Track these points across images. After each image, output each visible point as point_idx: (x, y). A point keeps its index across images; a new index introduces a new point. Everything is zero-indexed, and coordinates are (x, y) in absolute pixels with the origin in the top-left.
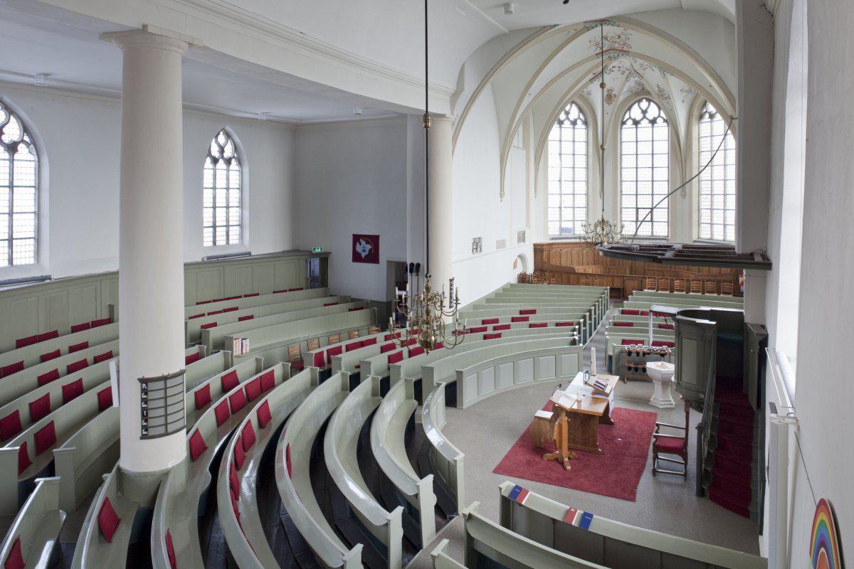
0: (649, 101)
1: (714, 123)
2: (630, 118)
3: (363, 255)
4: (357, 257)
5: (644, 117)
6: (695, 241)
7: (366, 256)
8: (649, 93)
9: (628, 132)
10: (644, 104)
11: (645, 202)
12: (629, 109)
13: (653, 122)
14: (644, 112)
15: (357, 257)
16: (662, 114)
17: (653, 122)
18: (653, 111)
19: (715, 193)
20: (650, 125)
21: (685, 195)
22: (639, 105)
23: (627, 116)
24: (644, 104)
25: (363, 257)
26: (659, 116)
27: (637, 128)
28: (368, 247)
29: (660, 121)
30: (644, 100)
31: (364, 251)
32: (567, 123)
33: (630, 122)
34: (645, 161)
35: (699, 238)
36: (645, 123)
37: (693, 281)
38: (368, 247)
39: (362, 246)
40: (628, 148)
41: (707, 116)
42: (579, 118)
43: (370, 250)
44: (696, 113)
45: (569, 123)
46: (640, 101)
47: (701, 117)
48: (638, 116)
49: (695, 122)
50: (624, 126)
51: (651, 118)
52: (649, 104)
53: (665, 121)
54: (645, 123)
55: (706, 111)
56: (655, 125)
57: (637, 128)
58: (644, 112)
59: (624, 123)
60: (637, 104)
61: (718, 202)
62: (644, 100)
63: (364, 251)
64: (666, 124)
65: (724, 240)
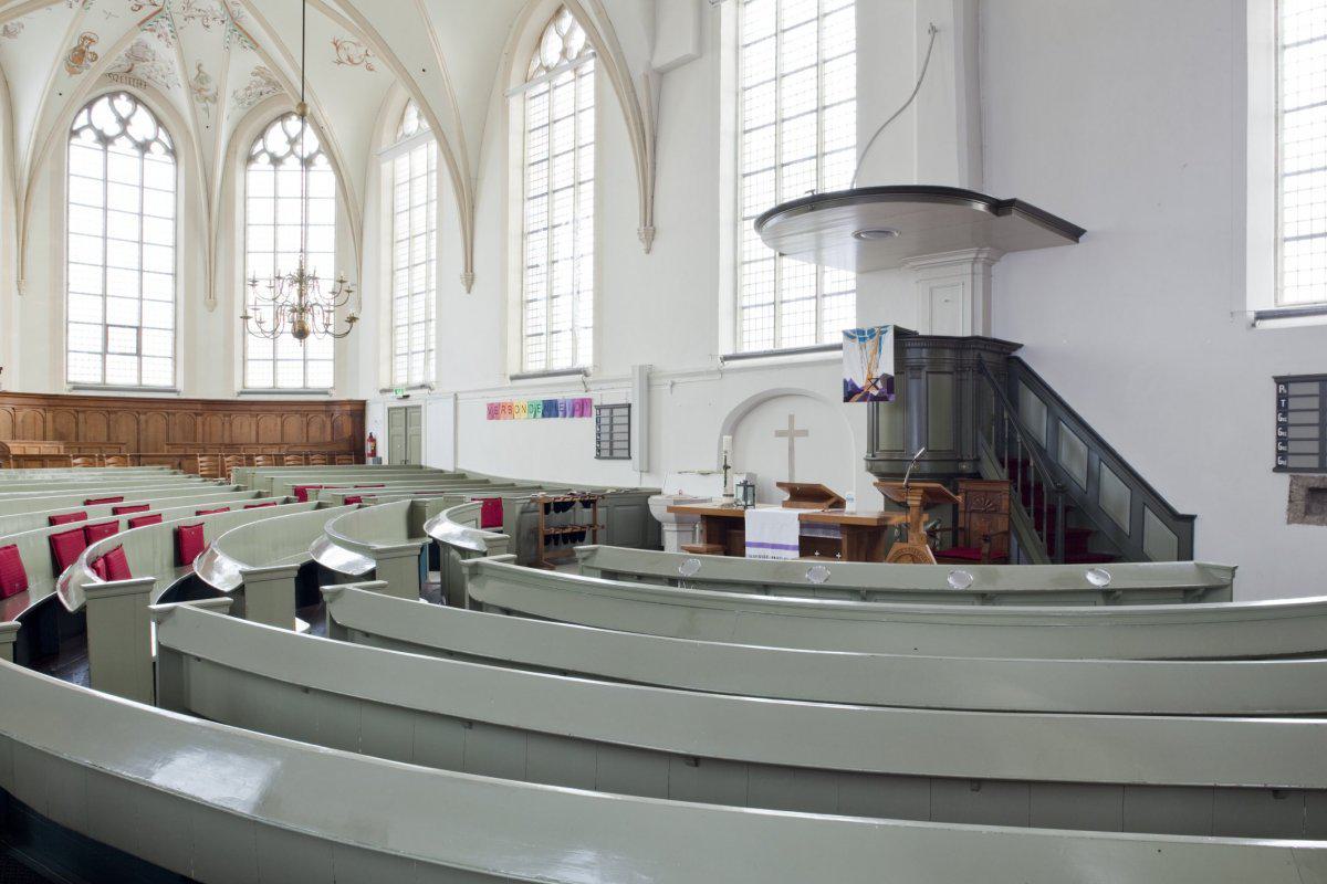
0: (136, 100)
1: (280, 174)
2: (90, 125)
5: (124, 132)
6: (242, 393)
8: (141, 84)
9: (82, 155)
10: (124, 105)
11: (122, 312)
12: (89, 105)
13: (144, 147)
14: (124, 122)
16: (162, 135)
17: (144, 147)
18: (143, 125)
20: (136, 153)
21: (215, 304)
22: (111, 104)
23: (82, 120)
26: (156, 139)
27: (105, 150)
29: (155, 147)
30: (123, 97)
32: (292, 163)
33: (88, 137)
34: (124, 226)
35: (244, 387)
40: (82, 190)
41: (264, 159)
42: (156, 139)
44: (242, 149)
45: (130, 144)
46: (113, 95)
47: (250, 159)
48: (112, 128)
49: (239, 165)
50: (74, 141)
51: (140, 139)
52: (135, 110)
53: (173, 152)
54: (123, 145)
55: (264, 150)
56: (147, 155)
57: (105, 150)
58: (124, 122)
59: (74, 133)
60: (106, 100)
62: (123, 97)
64: (169, 159)
65: (274, 387)
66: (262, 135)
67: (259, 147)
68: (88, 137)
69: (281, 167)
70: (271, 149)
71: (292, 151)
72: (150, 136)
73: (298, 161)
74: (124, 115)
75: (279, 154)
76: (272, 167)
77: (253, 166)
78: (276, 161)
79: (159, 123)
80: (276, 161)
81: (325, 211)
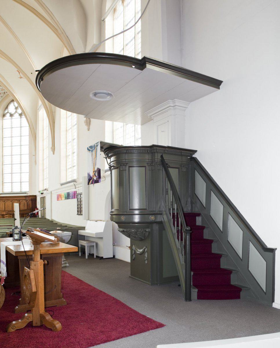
1: (13, 120)
19: (13, 163)
35: (3, 192)
37: (6, 215)
41: (8, 115)
47: (4, 116)
55: (8, 112)
61: (16, 168)
66: (7, 108)
67: (6, 111)
69: (13, 117)
70: (10, 112)
71: (16, 112)
73: (18, 115)
75: (13, 113)
76: (10, 118)
77: (5, 118)
78: (11, 115)
80: (11, 115)
81: (26, 130)
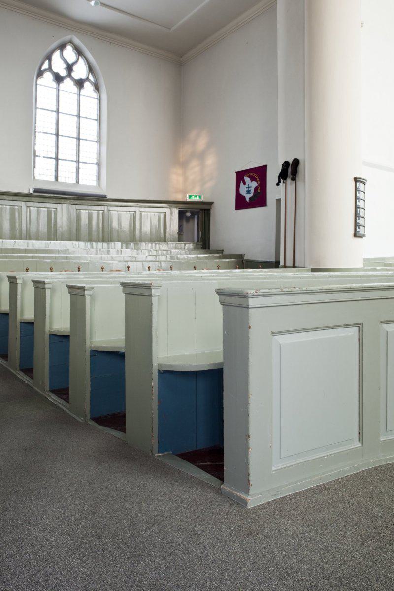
0: (79, 52)
3: (248, 197)
4: (241, 203)
5: (69, 75)
7: (251, 198)
14: (70, 68)
15: (241, 203)
16: (91, 78)
17: (80, 83)
18: (80, 70)
23: (45, 66)
24: (69, 53)
25: (247, 200)
28: (254, 184)
29: (87, 85)
31: (249, 192)
33: (48, 77)
36: (68, 84)
38: (254, 184)
39: (247, 186)
43: (256, 189)
46: (62, 47)
48: (61, 70)
50: (40, 81)
53: (97, 88)
54: (68, 84)
58: (70, 68)
60: (58, 53)
63: (249, 192)
64: (95, 95)
68: (48, 77)
72: (84, 77)
74: (70, 62)
79: (91, 69)
